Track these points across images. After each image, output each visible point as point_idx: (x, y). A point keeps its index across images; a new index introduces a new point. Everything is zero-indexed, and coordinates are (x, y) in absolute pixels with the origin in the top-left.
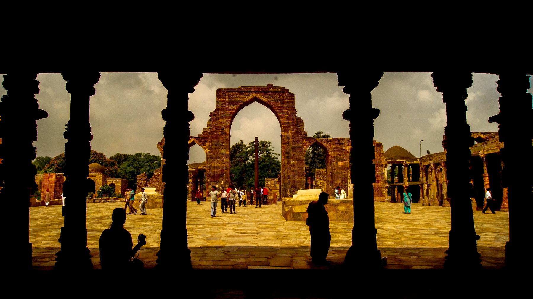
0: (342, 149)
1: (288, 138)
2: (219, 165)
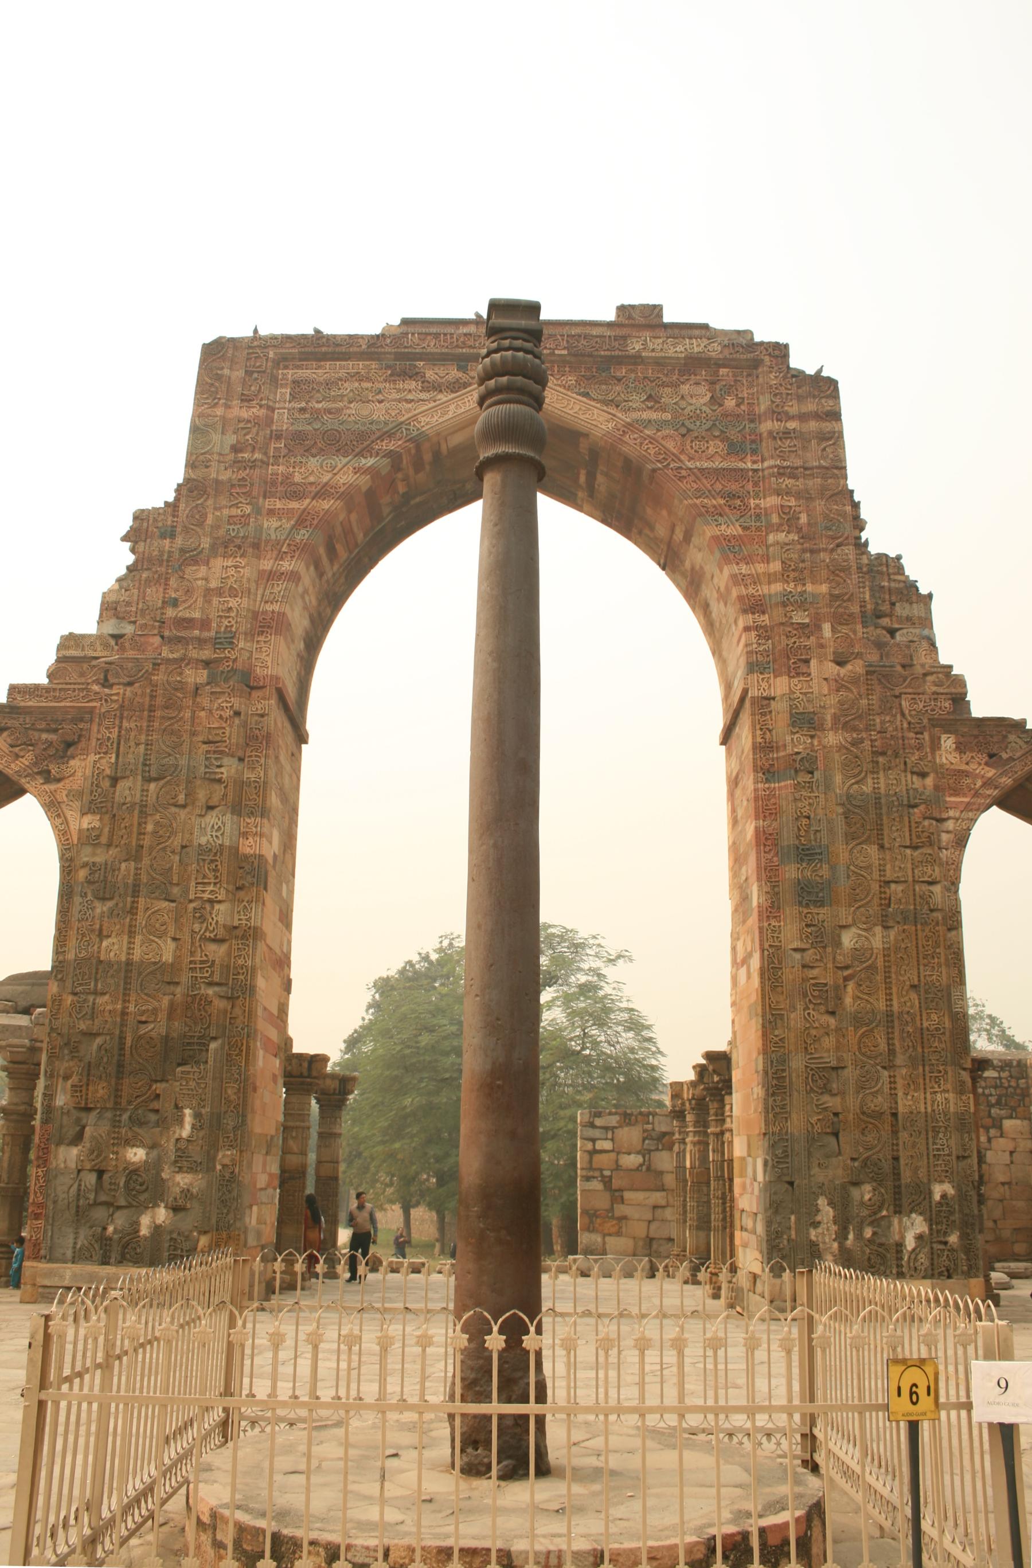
1: (805, 721)
2: (168, 952)
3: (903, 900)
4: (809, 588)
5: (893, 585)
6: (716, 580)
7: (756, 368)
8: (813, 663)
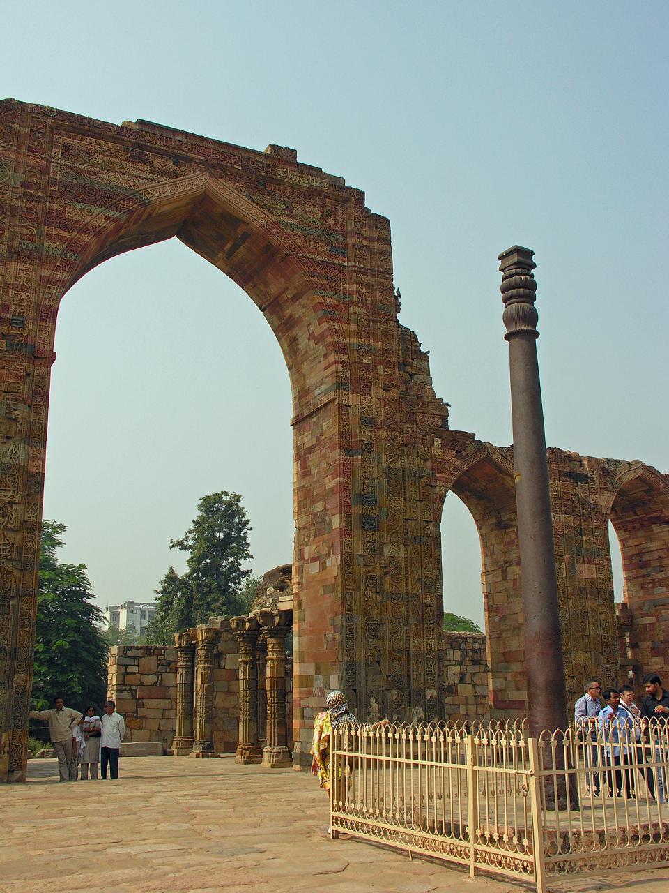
0: (585, 503)
1: (368, 422)
3: (415, 531)
4: (372, 343)
5: (413, 348)
6: (311, 328)
7: (346, 202)
8: (373, 388)
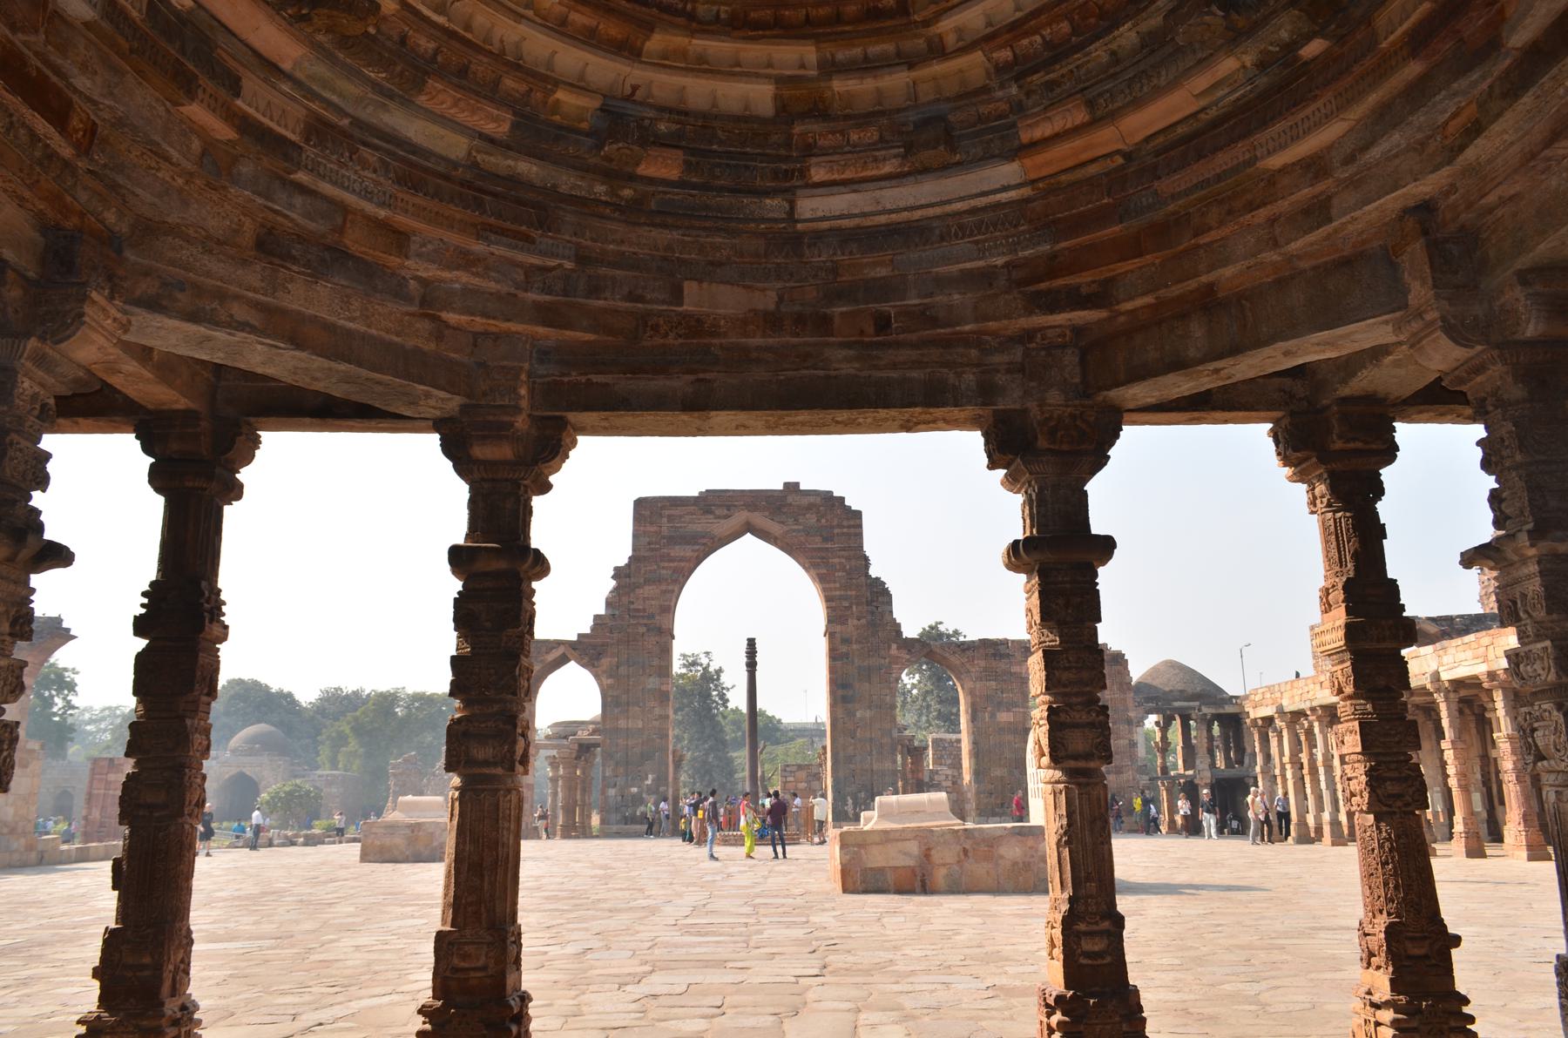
1: (846, 641)
